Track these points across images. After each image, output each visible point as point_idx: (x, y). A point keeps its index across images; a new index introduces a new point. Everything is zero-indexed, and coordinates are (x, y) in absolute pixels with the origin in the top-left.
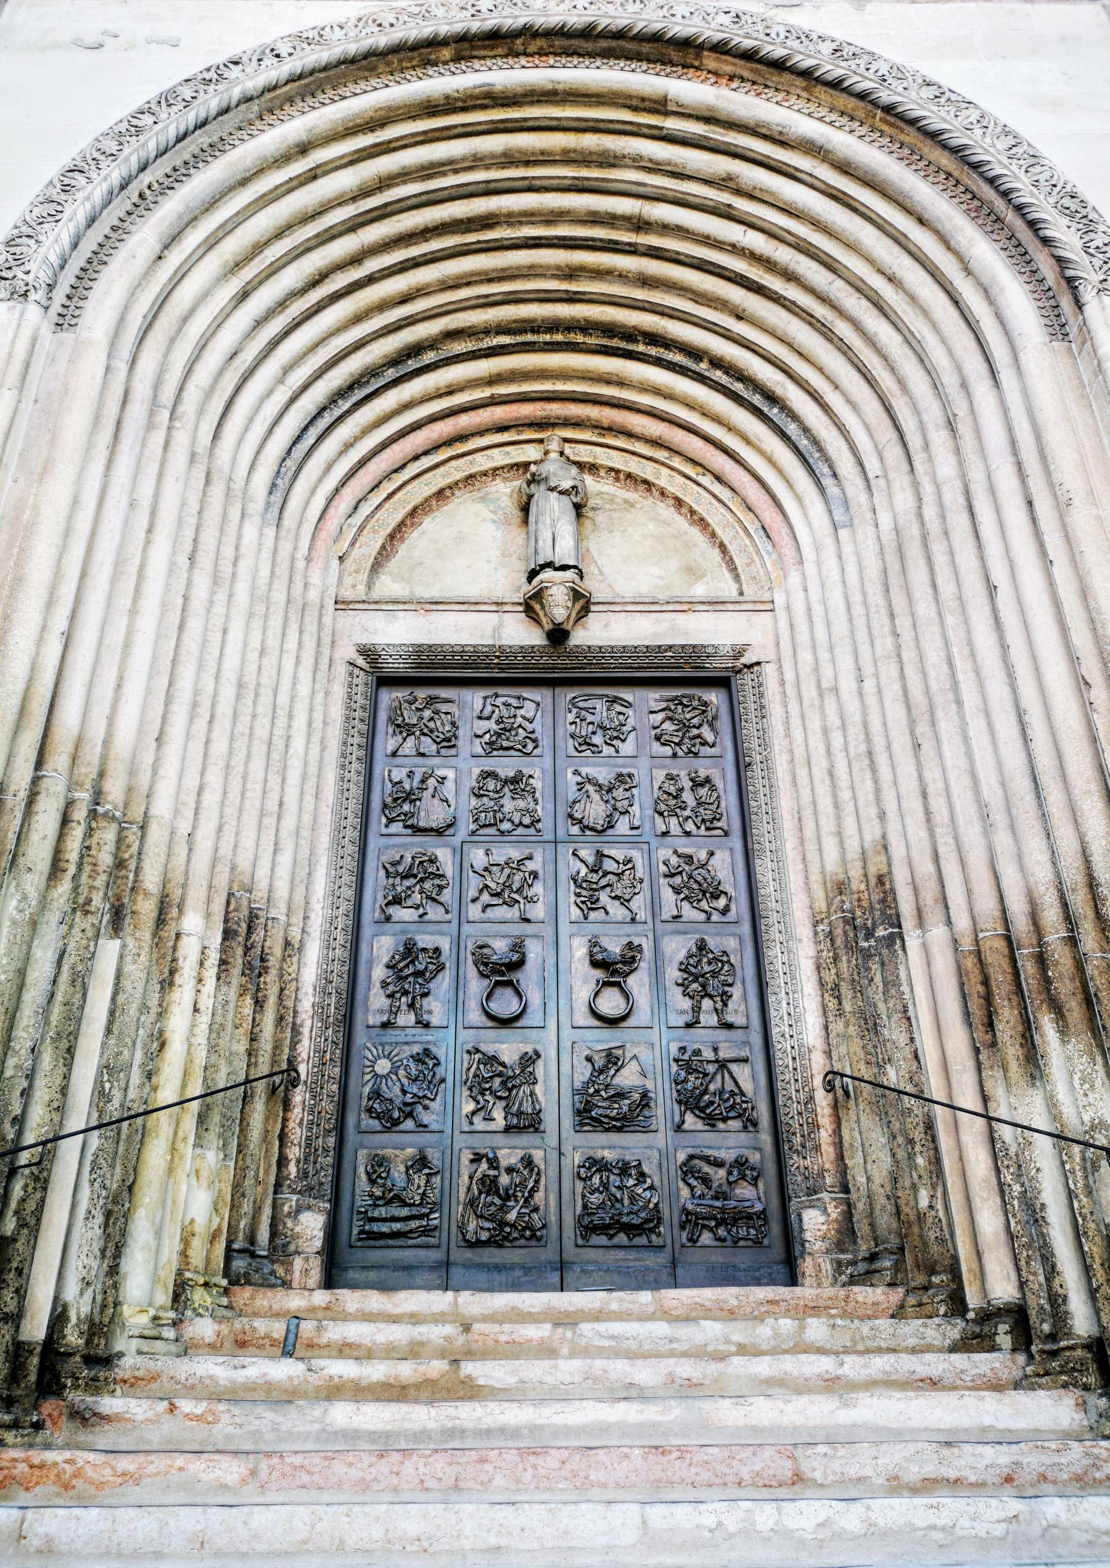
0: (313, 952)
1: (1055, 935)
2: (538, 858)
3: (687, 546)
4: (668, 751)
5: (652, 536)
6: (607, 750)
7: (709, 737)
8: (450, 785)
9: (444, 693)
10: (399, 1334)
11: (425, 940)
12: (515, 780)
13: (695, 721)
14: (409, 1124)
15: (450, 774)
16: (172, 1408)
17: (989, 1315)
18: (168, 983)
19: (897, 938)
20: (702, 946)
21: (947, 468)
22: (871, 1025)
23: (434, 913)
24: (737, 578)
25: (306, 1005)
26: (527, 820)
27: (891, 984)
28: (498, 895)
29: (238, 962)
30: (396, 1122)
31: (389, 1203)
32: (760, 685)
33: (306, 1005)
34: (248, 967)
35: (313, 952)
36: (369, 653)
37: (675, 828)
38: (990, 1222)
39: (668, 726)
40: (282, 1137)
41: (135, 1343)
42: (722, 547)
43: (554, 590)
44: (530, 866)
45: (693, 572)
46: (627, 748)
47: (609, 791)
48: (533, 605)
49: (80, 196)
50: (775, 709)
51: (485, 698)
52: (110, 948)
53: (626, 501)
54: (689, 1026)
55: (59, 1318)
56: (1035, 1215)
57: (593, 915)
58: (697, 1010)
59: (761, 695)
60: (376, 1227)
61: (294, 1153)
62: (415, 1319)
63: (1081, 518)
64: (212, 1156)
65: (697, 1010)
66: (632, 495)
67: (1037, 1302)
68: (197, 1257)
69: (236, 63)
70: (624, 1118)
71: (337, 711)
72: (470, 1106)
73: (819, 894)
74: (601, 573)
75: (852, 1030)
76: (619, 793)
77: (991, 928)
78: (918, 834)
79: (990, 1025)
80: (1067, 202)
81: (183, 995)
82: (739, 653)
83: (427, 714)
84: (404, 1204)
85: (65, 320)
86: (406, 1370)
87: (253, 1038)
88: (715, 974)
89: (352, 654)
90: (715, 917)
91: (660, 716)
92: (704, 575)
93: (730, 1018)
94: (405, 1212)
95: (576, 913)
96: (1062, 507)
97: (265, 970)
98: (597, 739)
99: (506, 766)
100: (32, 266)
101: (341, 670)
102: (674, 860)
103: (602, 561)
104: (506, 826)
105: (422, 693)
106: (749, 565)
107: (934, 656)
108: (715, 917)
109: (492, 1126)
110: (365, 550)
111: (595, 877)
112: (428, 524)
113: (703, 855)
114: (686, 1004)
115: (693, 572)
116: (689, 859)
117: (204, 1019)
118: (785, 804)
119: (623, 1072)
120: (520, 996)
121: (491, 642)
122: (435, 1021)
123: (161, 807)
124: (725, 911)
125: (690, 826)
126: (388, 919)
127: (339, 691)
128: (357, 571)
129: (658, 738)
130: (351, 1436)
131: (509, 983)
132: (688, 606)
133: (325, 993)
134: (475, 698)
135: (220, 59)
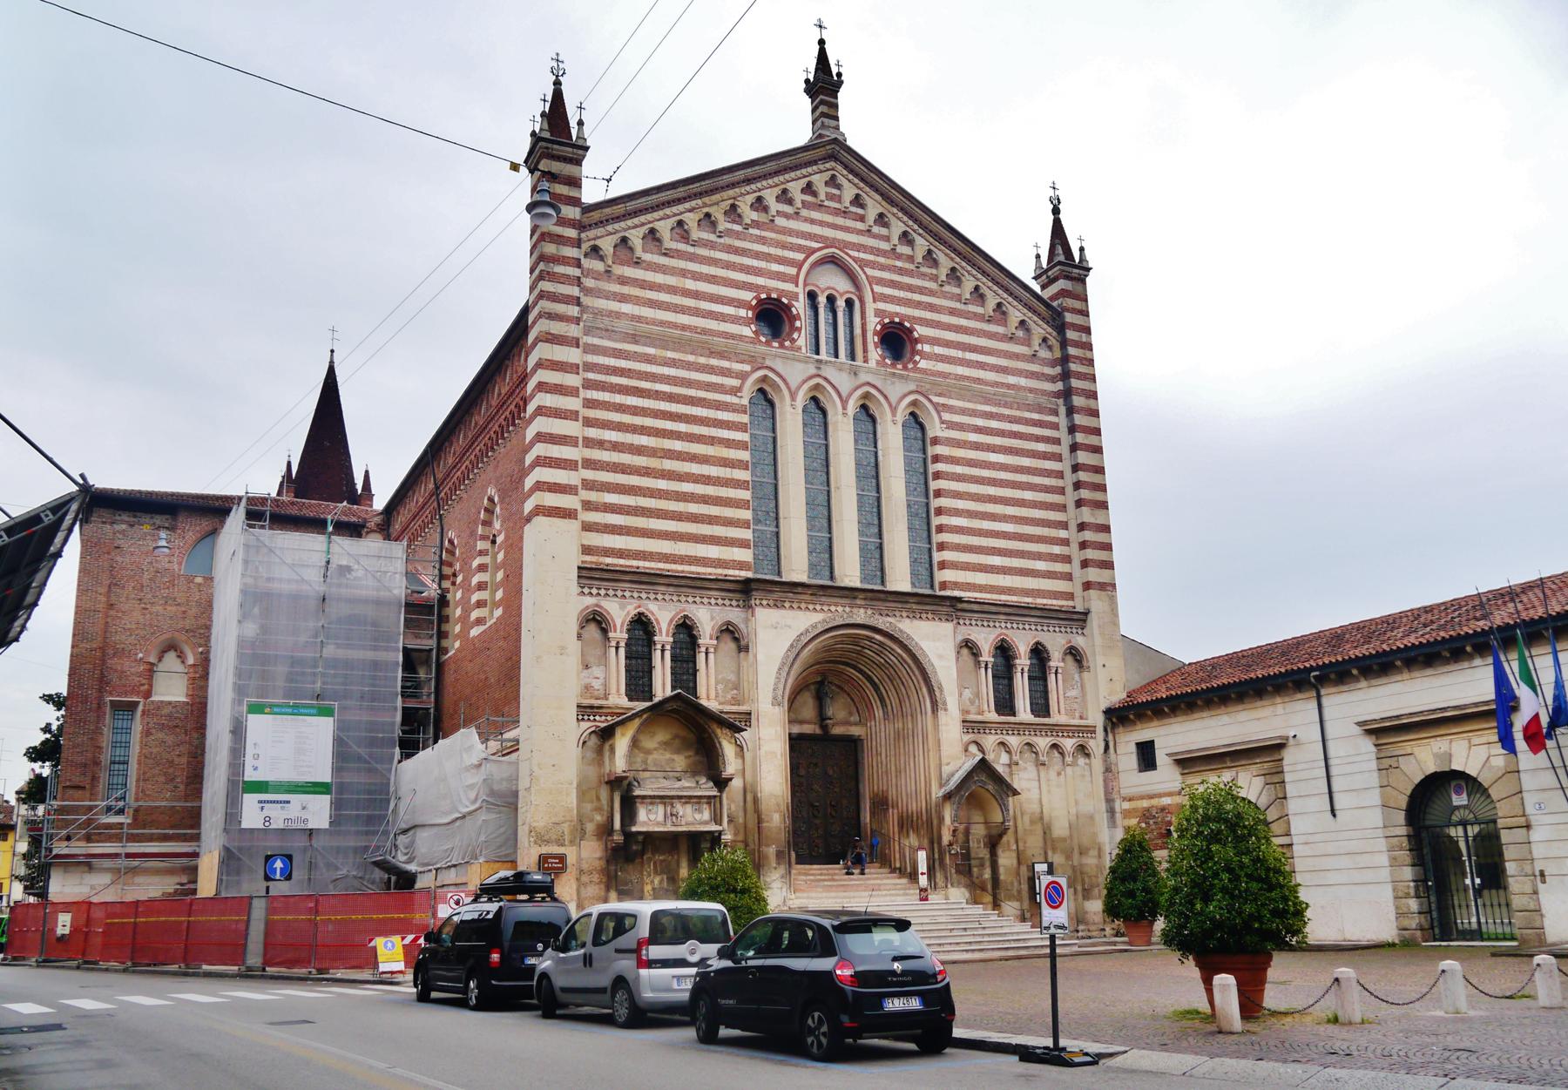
1: (915, 819)
17: (895, 869)
19: (888, 809)
21: (910, 726)
27: (885, 817)
38: (897, 856)
45: (851, 714)
56: (905, 857)
63: (931, 753)
67: (903, 869)
77: (905, 815)
78: (894, 792)
79: (902, 827)
96: (929, 751)
107: (902, 762)
115: (851, 714)
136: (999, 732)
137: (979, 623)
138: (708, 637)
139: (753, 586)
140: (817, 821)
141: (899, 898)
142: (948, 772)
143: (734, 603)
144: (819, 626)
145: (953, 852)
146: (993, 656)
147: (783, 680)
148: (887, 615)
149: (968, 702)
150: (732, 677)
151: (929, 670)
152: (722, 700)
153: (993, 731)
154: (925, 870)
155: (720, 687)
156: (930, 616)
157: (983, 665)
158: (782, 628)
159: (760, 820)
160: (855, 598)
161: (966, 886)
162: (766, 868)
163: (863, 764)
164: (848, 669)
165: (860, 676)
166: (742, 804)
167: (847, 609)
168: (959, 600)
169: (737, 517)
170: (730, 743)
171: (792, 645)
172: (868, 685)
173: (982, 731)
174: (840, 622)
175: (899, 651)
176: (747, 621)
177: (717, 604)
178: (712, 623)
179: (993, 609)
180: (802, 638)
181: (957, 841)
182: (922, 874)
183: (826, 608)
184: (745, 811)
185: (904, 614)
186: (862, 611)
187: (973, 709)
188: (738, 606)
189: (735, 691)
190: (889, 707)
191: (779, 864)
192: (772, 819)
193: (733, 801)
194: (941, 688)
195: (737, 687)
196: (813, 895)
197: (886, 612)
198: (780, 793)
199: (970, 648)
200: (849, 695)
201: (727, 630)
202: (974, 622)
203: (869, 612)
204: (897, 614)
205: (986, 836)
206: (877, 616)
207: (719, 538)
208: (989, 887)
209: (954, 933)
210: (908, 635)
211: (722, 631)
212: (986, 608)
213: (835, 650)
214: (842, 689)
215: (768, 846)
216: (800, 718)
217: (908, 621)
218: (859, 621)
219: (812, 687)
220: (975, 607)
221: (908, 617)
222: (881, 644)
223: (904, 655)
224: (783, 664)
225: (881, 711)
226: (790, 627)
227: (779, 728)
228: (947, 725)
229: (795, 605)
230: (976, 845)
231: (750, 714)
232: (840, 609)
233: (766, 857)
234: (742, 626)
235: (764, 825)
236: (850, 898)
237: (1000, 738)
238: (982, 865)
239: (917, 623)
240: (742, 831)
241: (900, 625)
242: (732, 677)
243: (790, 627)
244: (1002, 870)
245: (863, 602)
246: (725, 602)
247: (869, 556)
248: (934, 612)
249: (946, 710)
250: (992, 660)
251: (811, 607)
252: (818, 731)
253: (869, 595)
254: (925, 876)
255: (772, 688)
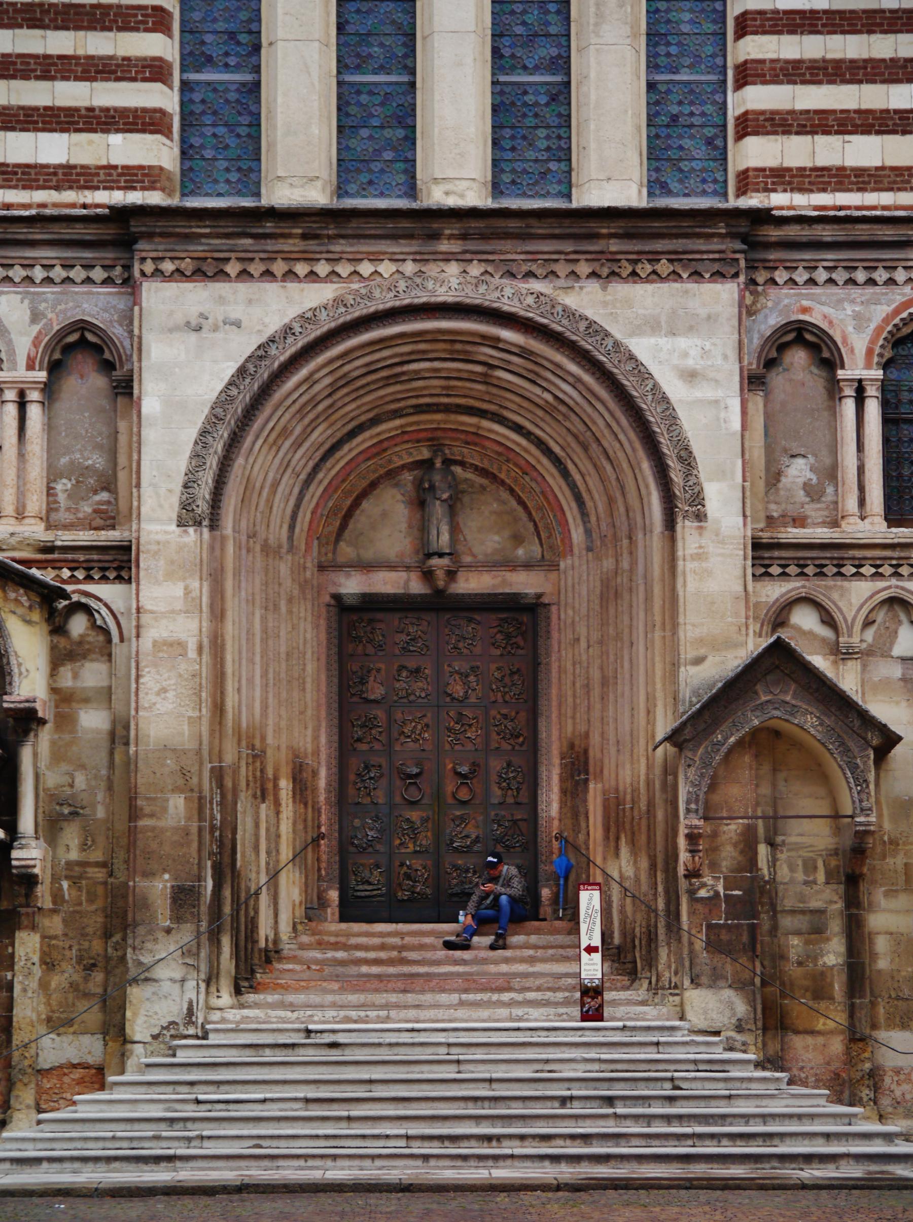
0: (323, 773)
2: (429, 715)
3: (516, 520)
4: (498, 652)
5: (495, 512)
6: (465, 651)
7: (522, 644)
8: (383, 672)
9: (379, 615)
10: (377, 941)
11: (374, 760)
12: (417, 671)
13: (514, 634)
14: (370, 850)
15: (382, 666)
16: (309, 968)
18: (278, 813)
20: (509, 765)
22: (575, 815)
23: (377, 746)
24: (541, 545)
25: (322, 798)
26: (423, 695)
28: (409, 737)
29: (298, 792)
30: (365, 849)
31: (363, 884)
32: (549, 618)
33: (322, 798)
34: (301, 790)
35: (323, 773)
36: (337, 597)
37: (500, 700)
39: (499, 637)
40: (318, 860)
41: (287, 946)
42: (535, 525)
43: (438, 572)
44: (425, 720)
45: (518, 539)
46: (478, 650)
47: (467, 676)
48: (428, 575)
49: (212, 451)
50: (555, 635)
51: (400, 619)
52: (263, 806)
53: (481, 486)
54: (500, 804)
55: (267, 940)
57: (456, 747)
58: (505, 796)
59: (549, 625)
60: (359, 894)
61: (323, 865)
62: (381, 935)
64: (297, 874)
65: (505, 796)
66: (484, 481)
68: (297, 914)
69: (273, 341)
70: (468, 847)
71: (323, 636)
72: (397, 842)
73: (565, 744)
74: (465, 540)
75: (569, 815)
76: (472, 678)
80: (683, 453)
81: (283, 816)
82: (539, 596)
83: (369, 628)
84: (370, 884)
85: (214, 525)
86: (383, 955)
87: (305, 820)
88: (514, 778)
89: (327, 599)
90: (517, 748)
91: (495, 630)
92: (523, 542)
93: (519, 800)
94: (370, 887)
95: (447, 747)
97: (306, 789)
98: (461, 645)
99: (412, 664)
100: (199, 502)
101: (324, 610)
102: (498, 717)
103: (466, 531)
104: (412, 698)
105: (367, 616)
106: (549, 537)
108: (517, 748)
109: (408, 850)
110: (330, 528)
111: (458, 727)
112: (365, 504)
113: (513, 714)
114: (499, 792)
115: (518, 539)
116: (505, 716)
117: (291, 821)
118: (554, 691)
119: (469, 826)
120: (420, 790)
121: (402, 591)
122: (380, 801)
123: (270, 740)
124: (521, 745)
125: (507, 698)
126: (355, 749)
127: (323, 622)
128: (327, 543)
129: (493, 644)
130: (368, 975)
131: (415, 783)
132: (511, 565)
133: (330, 792)
134: (394, 619)
135: (263, 339)
136: (887, 570)
137: (840, 276)
138: (22, 361)
139: (136, 226)
140: (415, 815)
141: (534, 1012)
142: (696, 682)
143: (98, 274)
144: (323, 315)
145: (703, 893)
146: (886, 366)
147: (213, 462)
148: (530, 274)
149: (801, 495)
150: (97, 460)
151: (653, 416)
152: (63, 516)
153: (867, 570)
154: (597, 942)
155: (62, 486)
156: (664, 267)
157: (849, 391)
158: (215, 329)
159: (134, 813)
160: (435, 236)
161: (740, 985)
162: (141, 930)
163: (549, 671)
164: (486, 423)
165: (524, 442)
166: (104, 772)
167: (409, 268)
168: (762, 216)
169: (121, 53)
170: (28, 622)
171: (242, 371)
172: (545, 461)
173: (830, 570)
174: (384, 301)
175: (573, 368)
176: (128, 319)
177: (48, 280)
178: (36, 328)
179: (887, 233)
180: (273, 351)
181: (714, 866)
182: (590, 950)
183: (344, 269)
184: (110, 788)
185: (584, 269)
186: (453, 269)
187: (813, 511)
188: (107, 281)
189: (104, 496)
190: (593, 519)
191: (178, 918)
192: (165, 809)
193: (83, 767)
194: (687, 459)
195: (108, 483)
196: (291, 998)
197: (525, 268)
198: (194, 745)
199: (814, 348)
200: (512, 491)
201: (82, 342)
202: (821, 275)
203: (475, 270)
204: (562, 269)
205: (836, 852)
206: (496, 280)
207: (71, 112)
208: (838, 988)
209: (576, 1109)
210: (591, 323)
211: (68, 349)
212: (862, 232)
213: (417, 376)
214: (493, 477)
215: (149, 874)
216: (368, 555)
217: (593, 286)
218: (443, 295)
219: (408, 477)
220: (827, 233)
221: (594, 275)
222: (525, 353)
223: (587, 378)
224: (214, 419)
225: (581, 530)
226: (237, 324)
227: (196, 584)
228: (700, 557)
229: (256, 268)
230: (800, 876)
231: (129, 548)
232: (386, 268)
233: (144, 904)
234: (117, 332)
235: (141, 823)
236: (386, 1006)
237: (888, 586)
238: (817, 931)
239: (621, 290)
240: (101, 840)
241: (570, 300)
242: (97, 460)
243: (237, 324)
244: (882, 944)
245: (454, 246)
246: (72, 274)
247: (530, 121)
248: (675, 257)
249: (700, 517)
250: (879, 374)
251: (301, 269)
252: (417, 587)
253: (475, 224)
254: (597, 957)
255: (180, 479)
